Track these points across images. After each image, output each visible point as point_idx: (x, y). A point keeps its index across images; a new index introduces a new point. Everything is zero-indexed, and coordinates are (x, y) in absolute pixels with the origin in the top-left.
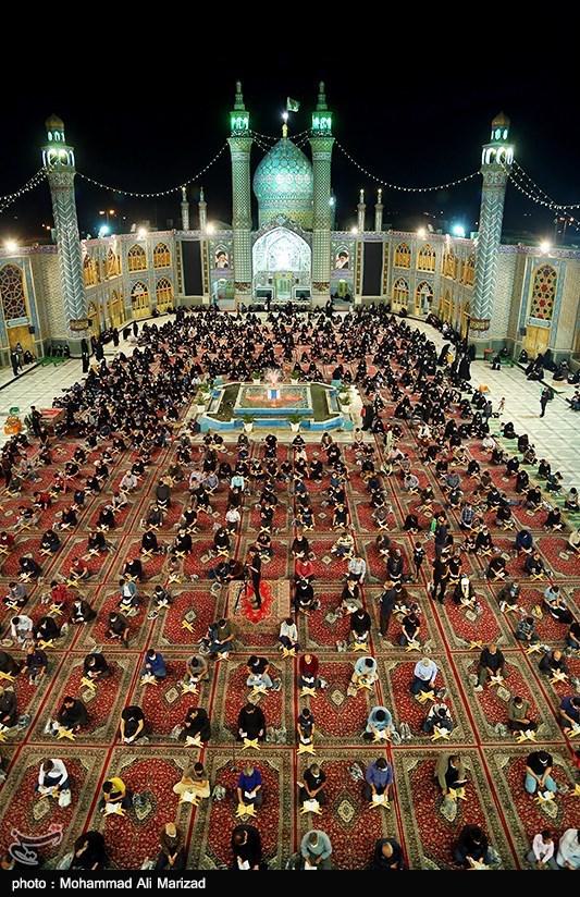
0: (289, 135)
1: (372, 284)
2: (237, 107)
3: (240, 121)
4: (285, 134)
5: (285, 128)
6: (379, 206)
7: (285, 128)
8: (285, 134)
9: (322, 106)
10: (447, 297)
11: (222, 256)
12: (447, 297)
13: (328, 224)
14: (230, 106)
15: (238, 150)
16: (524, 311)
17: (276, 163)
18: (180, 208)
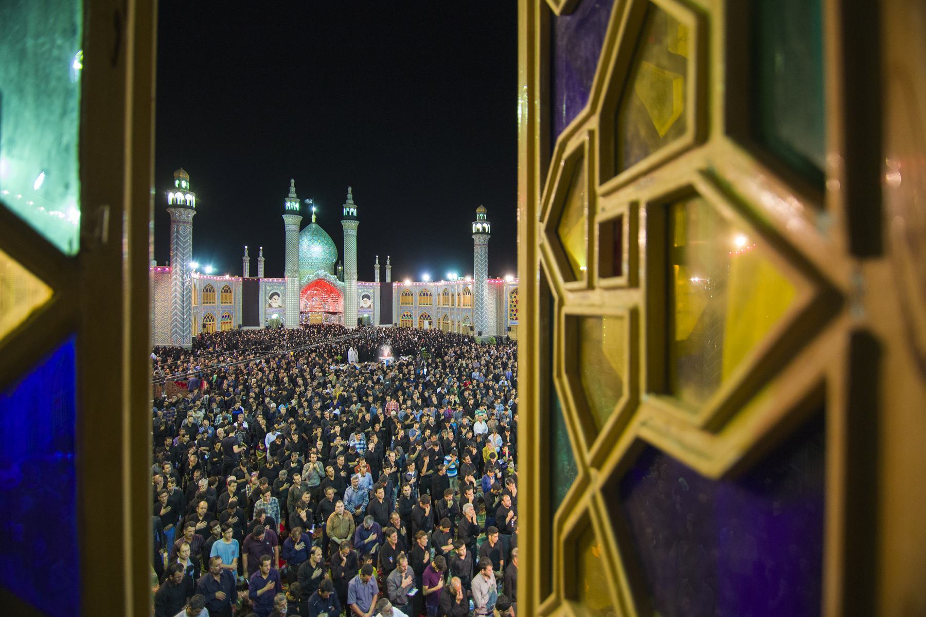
0: (317, 221)
1: (386, 316)
2: (290, 195)
3: (293, 204)
4: (314, 220)
5: (314, 217)
6: (388, 267)
7: (314, 217)
8: (314, 220)
9: (352, 202)
10: (445, 317)
11: (276, 297)
12: (445, 317)
13: (356, 277)
14: (286, 194)
15: (291, 222)
16: (506, 316)
17: (309, 237)
18: (242, 262)
